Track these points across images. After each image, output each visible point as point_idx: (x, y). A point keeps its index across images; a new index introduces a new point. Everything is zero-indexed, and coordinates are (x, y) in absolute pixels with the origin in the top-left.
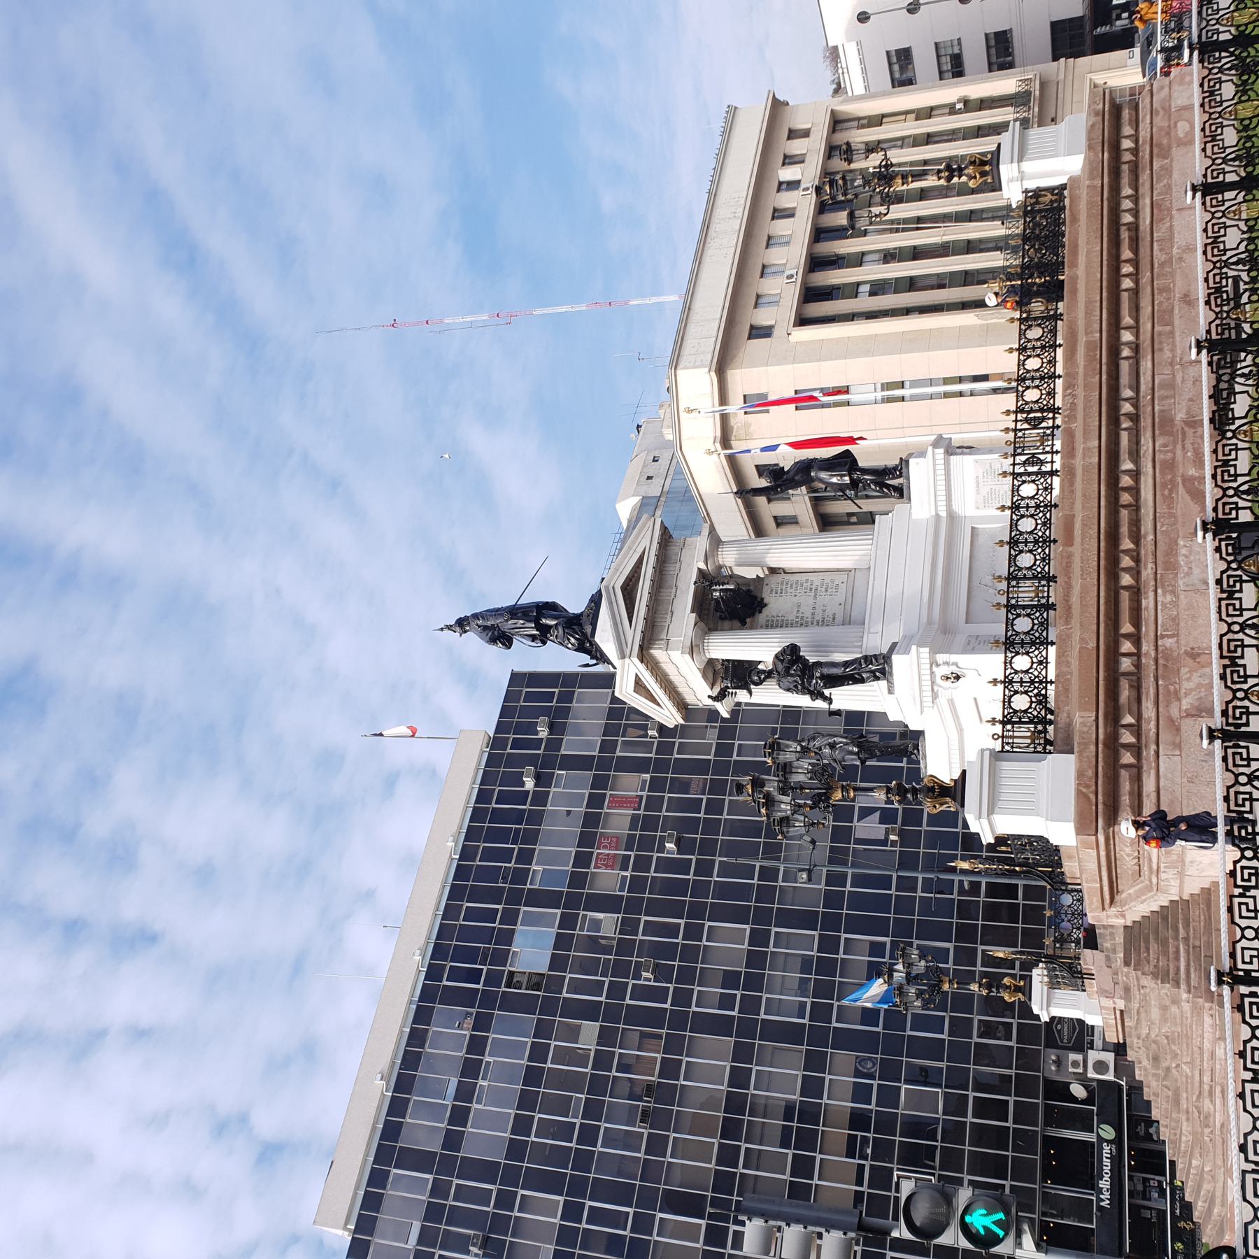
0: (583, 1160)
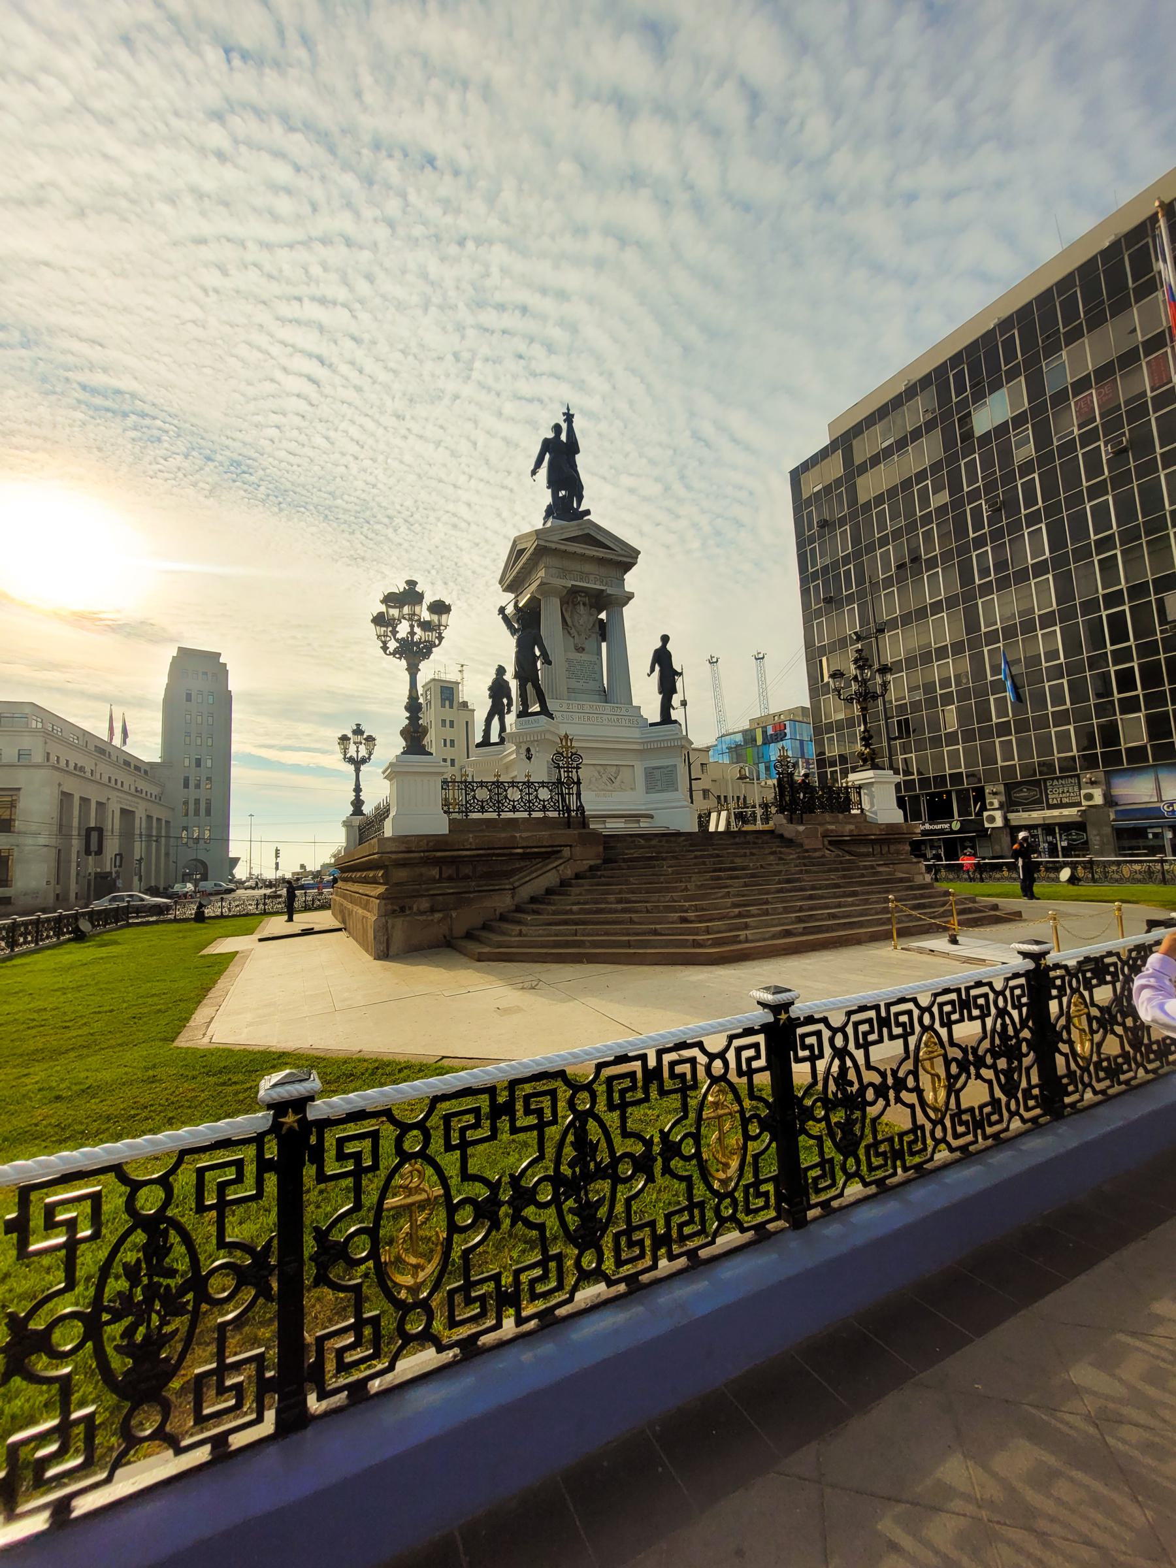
0: (871, 548)
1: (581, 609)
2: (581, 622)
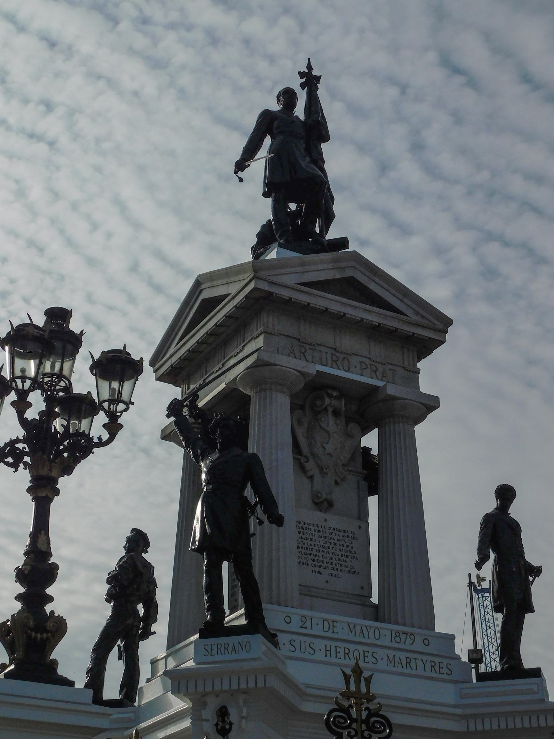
1: (330, 423)
2: (329, 448)
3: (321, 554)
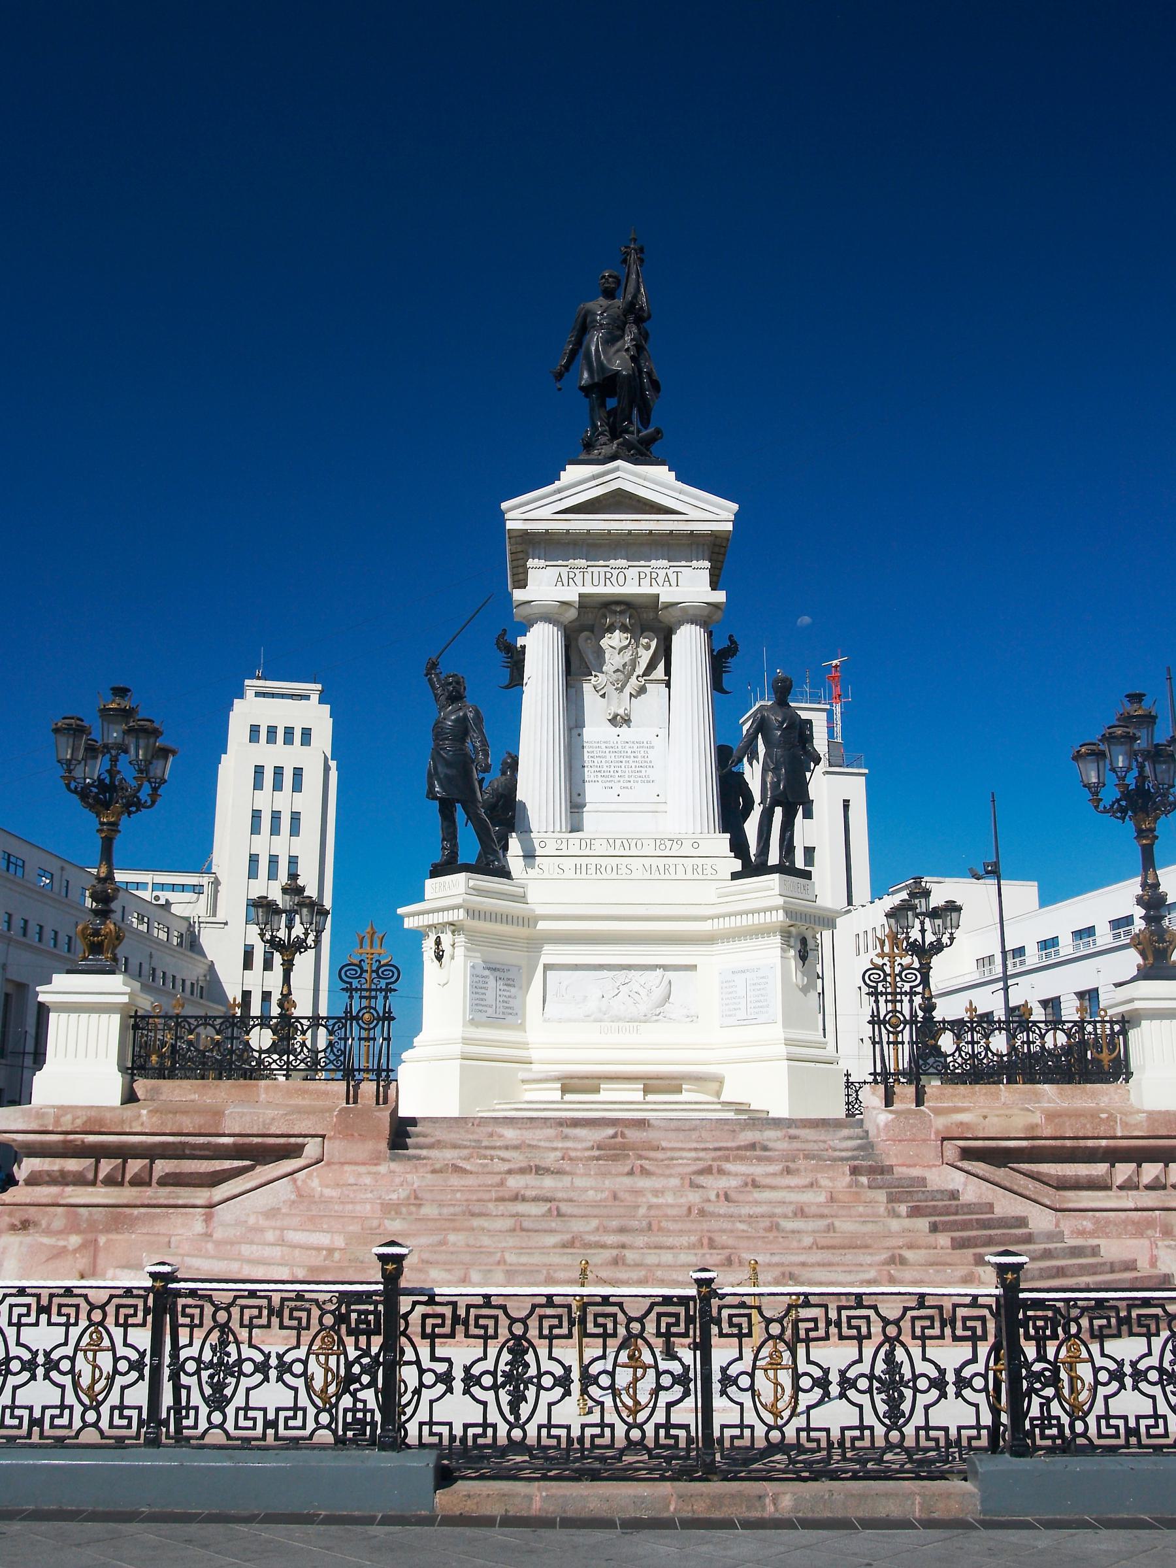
3: (612, 769)
